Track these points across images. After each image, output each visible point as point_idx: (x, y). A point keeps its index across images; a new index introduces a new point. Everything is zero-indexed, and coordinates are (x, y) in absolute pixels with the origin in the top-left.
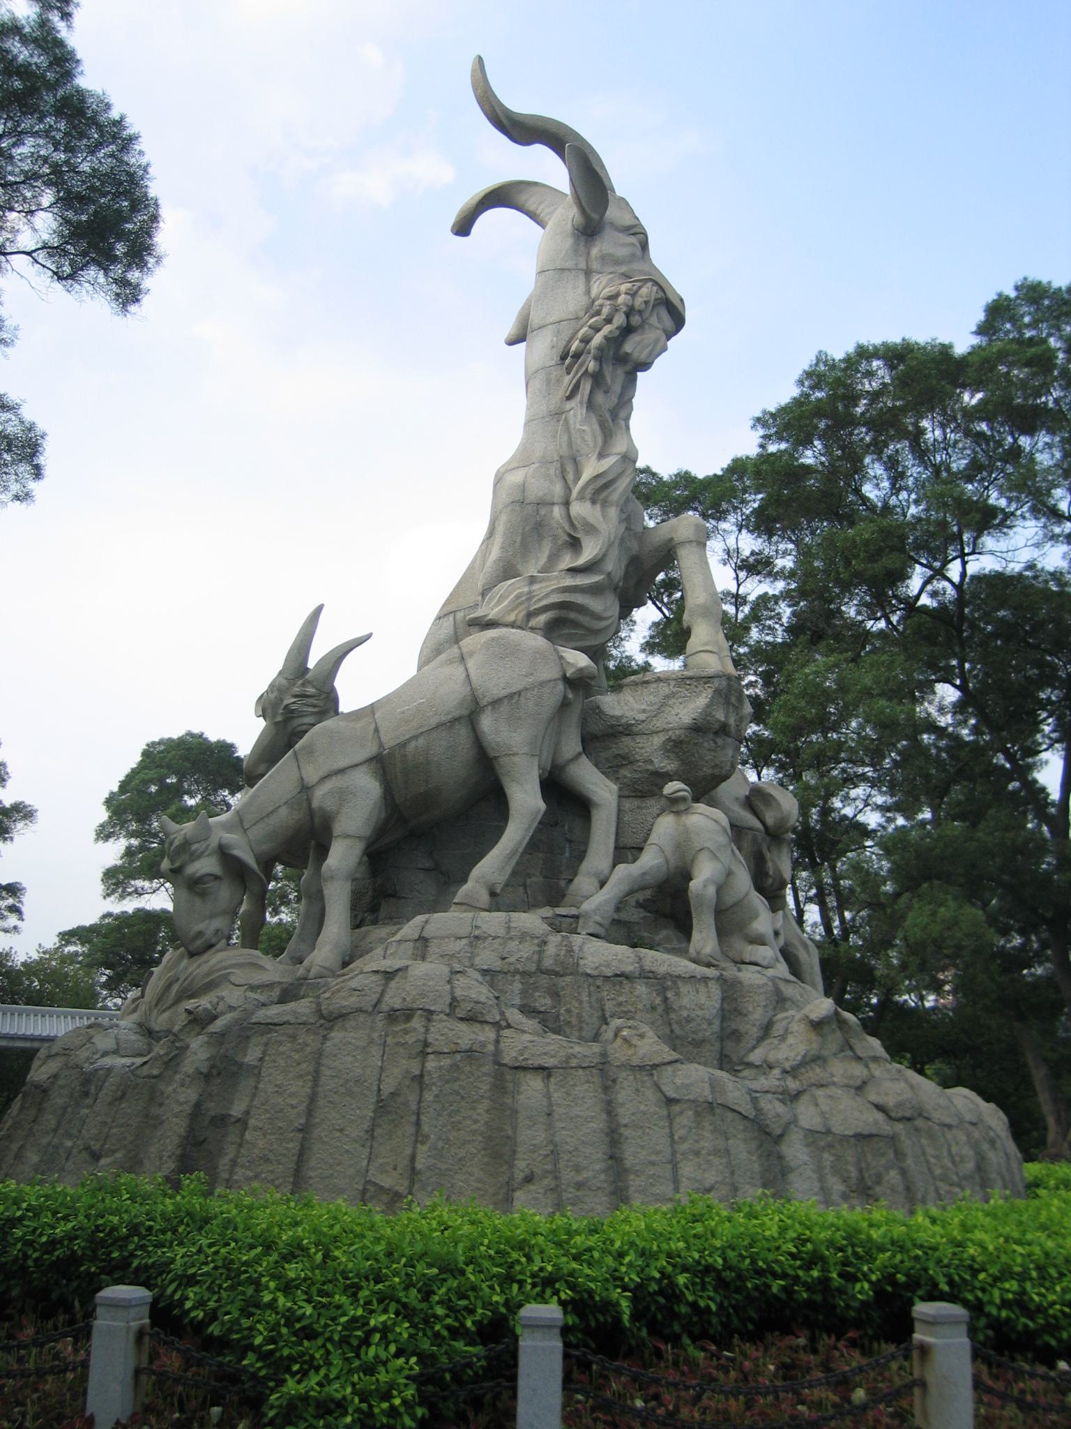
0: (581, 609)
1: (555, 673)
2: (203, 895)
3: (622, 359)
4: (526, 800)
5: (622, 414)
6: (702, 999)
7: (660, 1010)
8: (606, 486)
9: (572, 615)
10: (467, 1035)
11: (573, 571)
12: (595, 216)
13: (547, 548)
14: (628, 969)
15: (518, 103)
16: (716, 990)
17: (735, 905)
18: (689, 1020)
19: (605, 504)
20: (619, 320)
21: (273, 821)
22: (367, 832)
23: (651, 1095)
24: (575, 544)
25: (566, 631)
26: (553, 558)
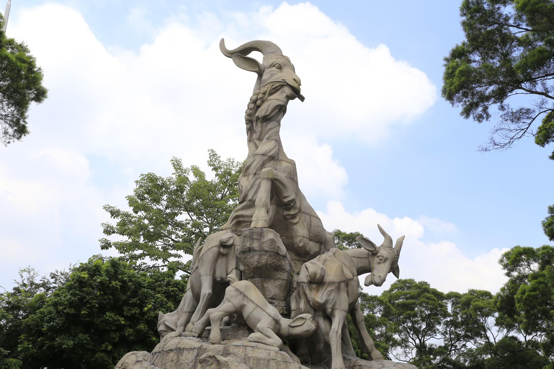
0: (242, 216)
1: (217, 243)
3: (258, 118)
5: (267, 136)
7: (175, 361)
9: (241, 219)
12: (257, 69)
14: (172, 347)
15: (233, 45)
17: (248, 316)
18: (182, 364)
19: (249, 174)
25: (243, 225)
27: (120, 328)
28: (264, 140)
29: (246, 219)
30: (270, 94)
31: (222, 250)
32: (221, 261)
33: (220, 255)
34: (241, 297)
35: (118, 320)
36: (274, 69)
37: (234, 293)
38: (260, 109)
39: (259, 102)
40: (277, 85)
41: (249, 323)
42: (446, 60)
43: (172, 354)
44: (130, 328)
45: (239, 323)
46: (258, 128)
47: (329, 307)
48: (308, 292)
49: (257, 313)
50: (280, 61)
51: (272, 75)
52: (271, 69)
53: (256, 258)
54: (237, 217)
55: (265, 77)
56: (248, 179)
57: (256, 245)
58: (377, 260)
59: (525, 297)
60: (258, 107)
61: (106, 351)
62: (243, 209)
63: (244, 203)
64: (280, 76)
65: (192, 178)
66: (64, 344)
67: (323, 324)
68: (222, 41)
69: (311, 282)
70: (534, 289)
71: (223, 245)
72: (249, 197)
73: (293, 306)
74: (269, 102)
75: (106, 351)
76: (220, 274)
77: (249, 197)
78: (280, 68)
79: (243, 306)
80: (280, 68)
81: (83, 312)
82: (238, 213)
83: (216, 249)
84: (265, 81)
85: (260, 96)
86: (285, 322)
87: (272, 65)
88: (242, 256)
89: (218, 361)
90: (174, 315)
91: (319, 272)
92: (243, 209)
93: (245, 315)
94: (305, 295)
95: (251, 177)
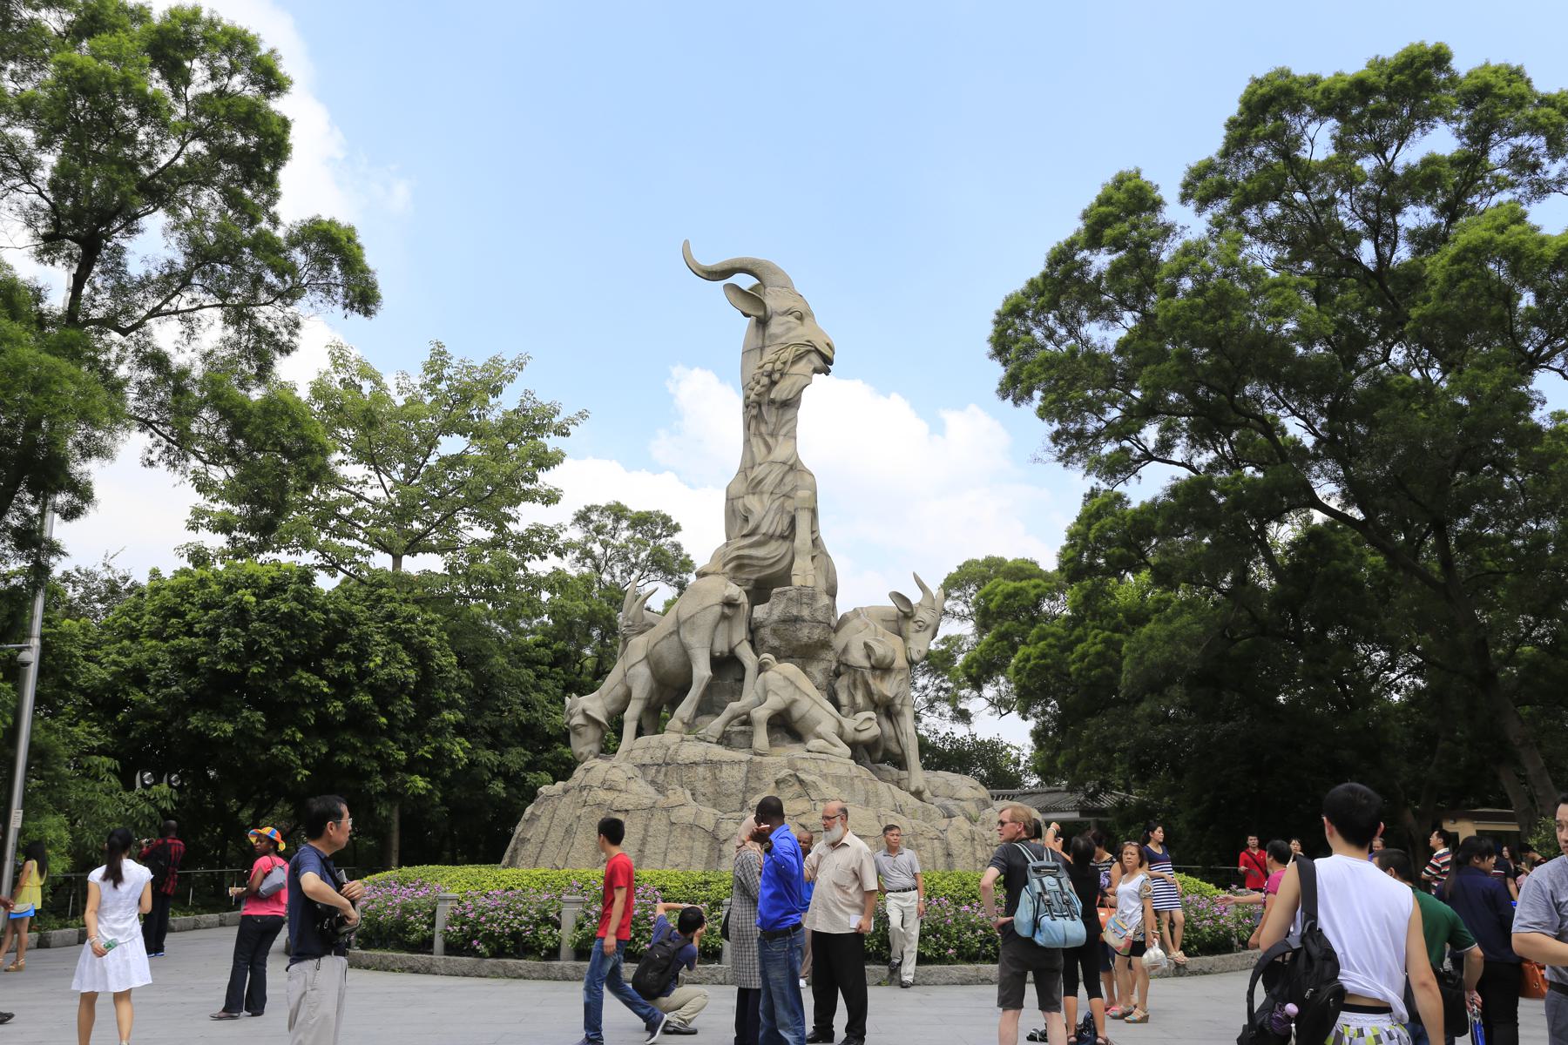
0: (750, 557)
1: (718, 599)
2: (579, 734)
3: (772, 402)
4: (702, 671)
5: (783, 431)
6: (734, 772)
8: (760, 482)
10: (602, 795)
11: (744, 536)
12: (761, 313)
13: (739, 522)
15: (712, 258)
16: (744, 768)
17: (803, 717)
19: (762, 493)
20: (765, 380)
21: (614, 693)
22: (644, 695)
23: (664, 821)
24: (746, 520)
26: (742, 528)
27: (322, 699)
28: (780, 438)
29: (754, 562)
30: (793, 363)
31: (726, 610)
32: (723, 626)
33: (724, 617)
34: (791, 689)
35: (317, 686)
36: (791, 318)
37: (782, 683)
38: (777, 387)
39: (776, 376)
40: (803, 349)
41: (799, 727)
42: (998, 314)
43: (701, 770)
44: (337, 699)
45: (786, 726)
46: (770, 415)
47: (898, 701)
48: (871, 681)
49: (816, 712)
50: (800, 307)
51: (789, 330)
52: (786, 319)
53: (806, 631)
54: (738, 557)
55: (775, 327)
56: (761, 501)
57: (806, 613)
58: (912, 626)
59: (1029, 666)
60: (774, 383)
61: (293, 744)
62: (751, 546)
63: (755, 538)
64: (801, 333)
65: (367, 386)
66: (215, 729)
67: (887, 726)
68: (686, 244)
69: (873, 668)
70: (1043, 656)
71: (730, 603)
72: (763, 530)
73: (844, 698)
74: (793, 379)
75: (293, 744)
76: (721, 646)
77: (763, 530)
78: (801, 318)
79: (794, 701)
80: (801, 318)
81: (255, 670)
82: (741, 552)
83: (718, 609)
84: (777, 336)
85: (778, 365)
86: (849, 724)
87: (788, 312)
88: (782, 627)
89: (801, 782)
90: (594, 700)
91: (890, 654)
92: (751, 546)
93: (796, 713)
94: (867, 685)
95: (766, 497)
